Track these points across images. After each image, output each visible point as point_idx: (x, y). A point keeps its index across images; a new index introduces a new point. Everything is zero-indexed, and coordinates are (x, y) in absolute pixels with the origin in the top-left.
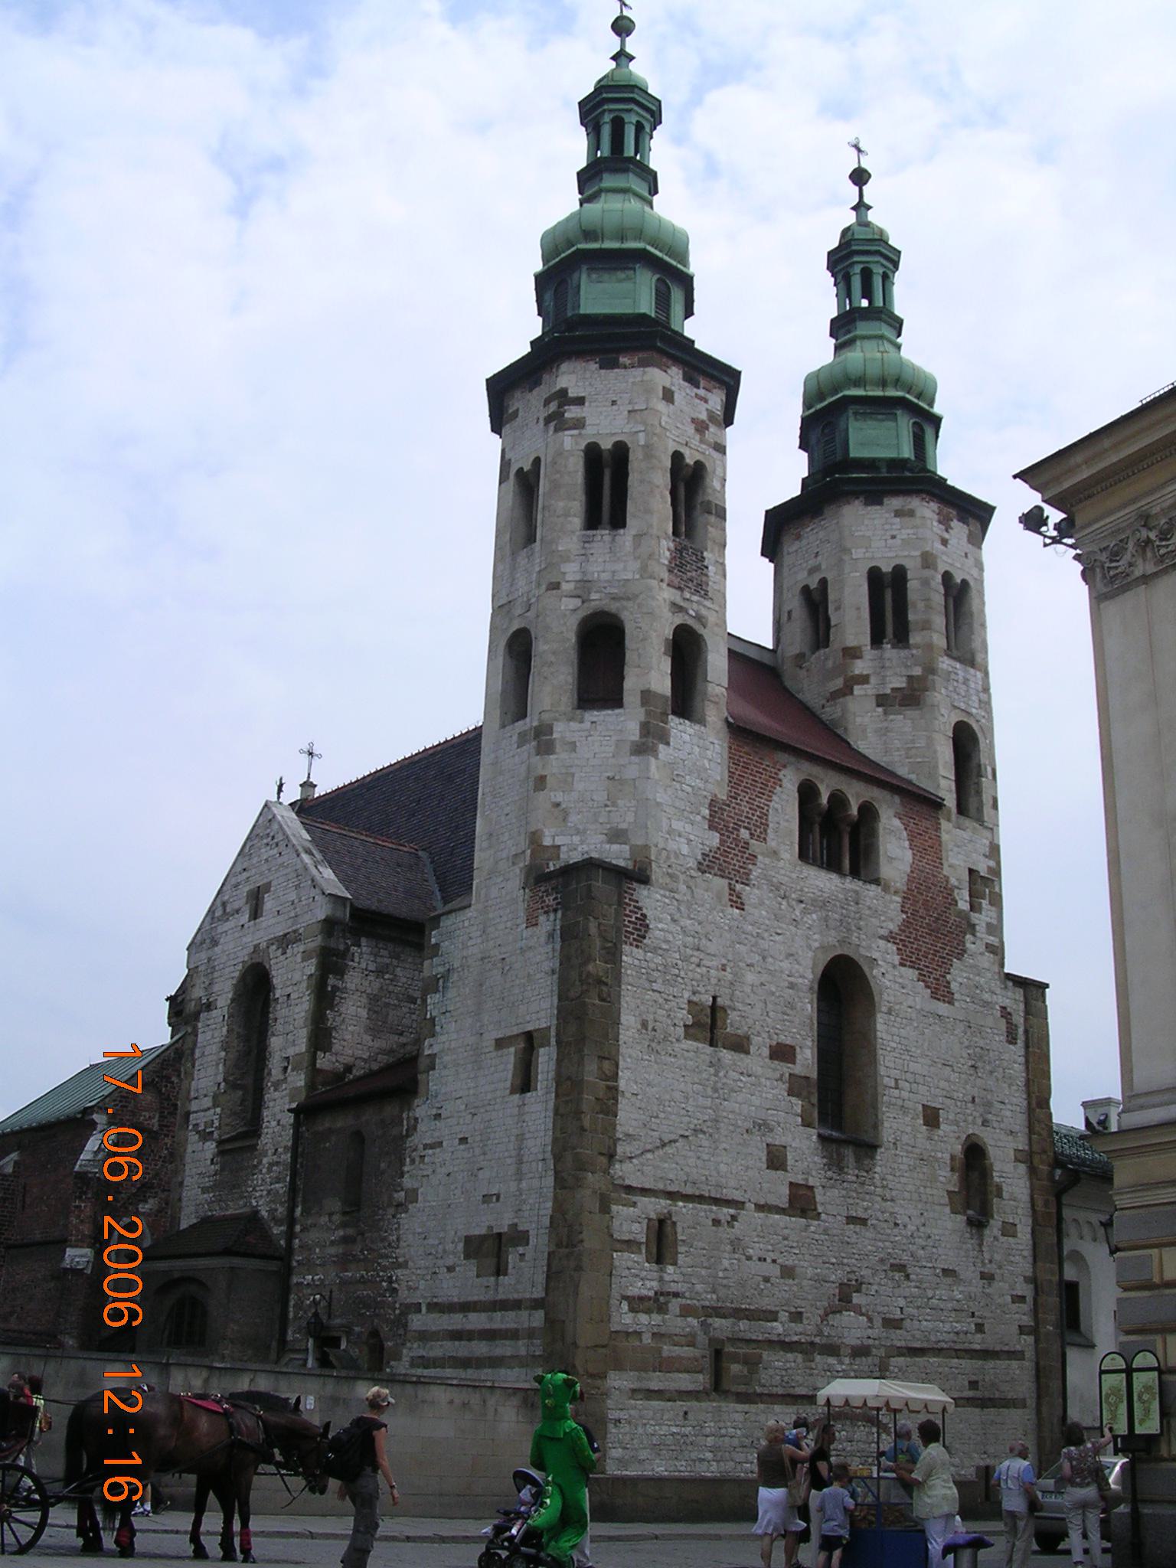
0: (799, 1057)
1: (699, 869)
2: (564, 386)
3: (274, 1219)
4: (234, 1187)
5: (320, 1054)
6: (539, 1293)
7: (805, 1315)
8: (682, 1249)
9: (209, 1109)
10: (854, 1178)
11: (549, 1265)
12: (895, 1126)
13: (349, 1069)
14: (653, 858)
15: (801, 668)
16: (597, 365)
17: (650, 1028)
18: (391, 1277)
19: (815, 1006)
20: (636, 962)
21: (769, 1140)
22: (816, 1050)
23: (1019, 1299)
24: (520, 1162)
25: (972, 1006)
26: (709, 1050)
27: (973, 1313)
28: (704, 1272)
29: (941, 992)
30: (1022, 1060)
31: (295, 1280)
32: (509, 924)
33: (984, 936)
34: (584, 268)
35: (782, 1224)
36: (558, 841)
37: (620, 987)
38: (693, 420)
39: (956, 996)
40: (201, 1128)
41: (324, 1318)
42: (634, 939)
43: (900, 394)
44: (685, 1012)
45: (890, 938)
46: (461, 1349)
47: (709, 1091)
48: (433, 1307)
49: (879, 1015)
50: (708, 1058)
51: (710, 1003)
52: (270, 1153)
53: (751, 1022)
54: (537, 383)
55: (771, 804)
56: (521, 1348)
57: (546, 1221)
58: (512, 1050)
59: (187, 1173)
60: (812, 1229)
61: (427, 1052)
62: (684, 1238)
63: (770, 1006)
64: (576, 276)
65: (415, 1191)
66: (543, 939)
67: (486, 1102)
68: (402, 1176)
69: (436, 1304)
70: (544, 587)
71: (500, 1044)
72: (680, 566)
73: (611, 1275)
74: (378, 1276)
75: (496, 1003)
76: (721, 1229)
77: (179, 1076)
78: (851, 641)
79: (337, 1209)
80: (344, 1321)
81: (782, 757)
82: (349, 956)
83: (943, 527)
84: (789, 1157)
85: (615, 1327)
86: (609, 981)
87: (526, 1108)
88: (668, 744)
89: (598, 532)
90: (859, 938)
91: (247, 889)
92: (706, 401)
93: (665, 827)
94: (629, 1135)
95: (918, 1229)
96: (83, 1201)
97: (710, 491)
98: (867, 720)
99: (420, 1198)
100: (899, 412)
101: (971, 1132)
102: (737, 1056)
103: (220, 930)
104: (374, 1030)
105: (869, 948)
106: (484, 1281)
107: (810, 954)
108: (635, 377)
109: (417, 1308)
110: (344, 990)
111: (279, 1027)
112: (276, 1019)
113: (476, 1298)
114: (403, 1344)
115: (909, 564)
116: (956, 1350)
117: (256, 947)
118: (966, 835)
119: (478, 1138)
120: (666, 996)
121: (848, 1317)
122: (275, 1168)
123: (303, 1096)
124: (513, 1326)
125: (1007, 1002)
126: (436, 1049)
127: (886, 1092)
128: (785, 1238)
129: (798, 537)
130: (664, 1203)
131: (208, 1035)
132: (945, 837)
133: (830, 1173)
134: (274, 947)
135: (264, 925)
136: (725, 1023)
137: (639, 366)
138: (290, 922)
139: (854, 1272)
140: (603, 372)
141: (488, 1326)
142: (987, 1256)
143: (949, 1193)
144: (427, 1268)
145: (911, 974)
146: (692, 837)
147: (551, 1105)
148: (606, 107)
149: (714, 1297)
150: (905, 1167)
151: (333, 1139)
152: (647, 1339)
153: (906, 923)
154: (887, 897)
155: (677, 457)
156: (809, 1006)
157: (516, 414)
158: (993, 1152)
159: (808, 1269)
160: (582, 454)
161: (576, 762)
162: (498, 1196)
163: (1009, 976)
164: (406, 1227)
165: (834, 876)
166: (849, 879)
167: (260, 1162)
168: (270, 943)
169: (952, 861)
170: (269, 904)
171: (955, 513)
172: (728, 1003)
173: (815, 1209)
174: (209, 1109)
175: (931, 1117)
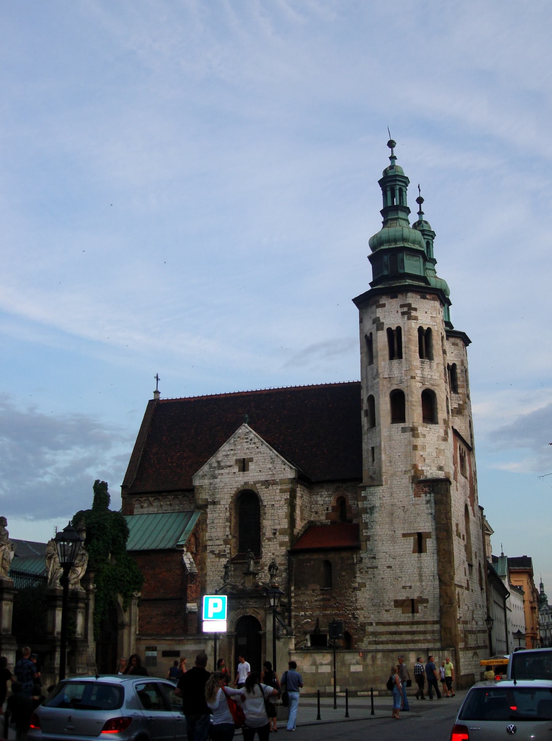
2: (410, 302)
6: (436, 619)
9: (221, 545)
11: (441, 611)
13: (298, 533)
16: (419, 297)
24: (420, 575)
30: (482, 534)
31: (293, 613)
32: (405, 495)
34: (405, 253)
36: (423, 469)
40: (217, 552)
46: (397, 638)
48: (378, 624)
54: (396, 297)
56: (429, 637)
57: (438, 596)
59: (208, 570)
61: (365, 534)
64: (400, 255)
66: (424, 502)
68: (355, 577)
69: (381, 622)
70: (409, 377)
71: (404, 535)
74: (346, 612)
75: (401, 521)
79: (317, 588)
87: (422, 558)
89: (426, 360)
91: (235, 458)
96: (192, 584)
99: (367, 586)
104: (302, 519)
106: (407, 615)
108: (432, 304)
109: (371, 624)
111: (268, 516)
112: (265, 513)
113: (403, 620)
114: (364, 637)
115: (457, 363)
117: (246, 483)
123: (289, 545)
126: (369, 534)
134: (260, 485)
141: (410, 630)
144: (375, 610)
151: (312, 562)
157: (384, 305)
159: (470, 608)
162: (410, 587)
163: (480, 507)
164: (360, 596)
167: (263, 568)
168: (255, 483)
170: (252, 466)
174: (221, 545)
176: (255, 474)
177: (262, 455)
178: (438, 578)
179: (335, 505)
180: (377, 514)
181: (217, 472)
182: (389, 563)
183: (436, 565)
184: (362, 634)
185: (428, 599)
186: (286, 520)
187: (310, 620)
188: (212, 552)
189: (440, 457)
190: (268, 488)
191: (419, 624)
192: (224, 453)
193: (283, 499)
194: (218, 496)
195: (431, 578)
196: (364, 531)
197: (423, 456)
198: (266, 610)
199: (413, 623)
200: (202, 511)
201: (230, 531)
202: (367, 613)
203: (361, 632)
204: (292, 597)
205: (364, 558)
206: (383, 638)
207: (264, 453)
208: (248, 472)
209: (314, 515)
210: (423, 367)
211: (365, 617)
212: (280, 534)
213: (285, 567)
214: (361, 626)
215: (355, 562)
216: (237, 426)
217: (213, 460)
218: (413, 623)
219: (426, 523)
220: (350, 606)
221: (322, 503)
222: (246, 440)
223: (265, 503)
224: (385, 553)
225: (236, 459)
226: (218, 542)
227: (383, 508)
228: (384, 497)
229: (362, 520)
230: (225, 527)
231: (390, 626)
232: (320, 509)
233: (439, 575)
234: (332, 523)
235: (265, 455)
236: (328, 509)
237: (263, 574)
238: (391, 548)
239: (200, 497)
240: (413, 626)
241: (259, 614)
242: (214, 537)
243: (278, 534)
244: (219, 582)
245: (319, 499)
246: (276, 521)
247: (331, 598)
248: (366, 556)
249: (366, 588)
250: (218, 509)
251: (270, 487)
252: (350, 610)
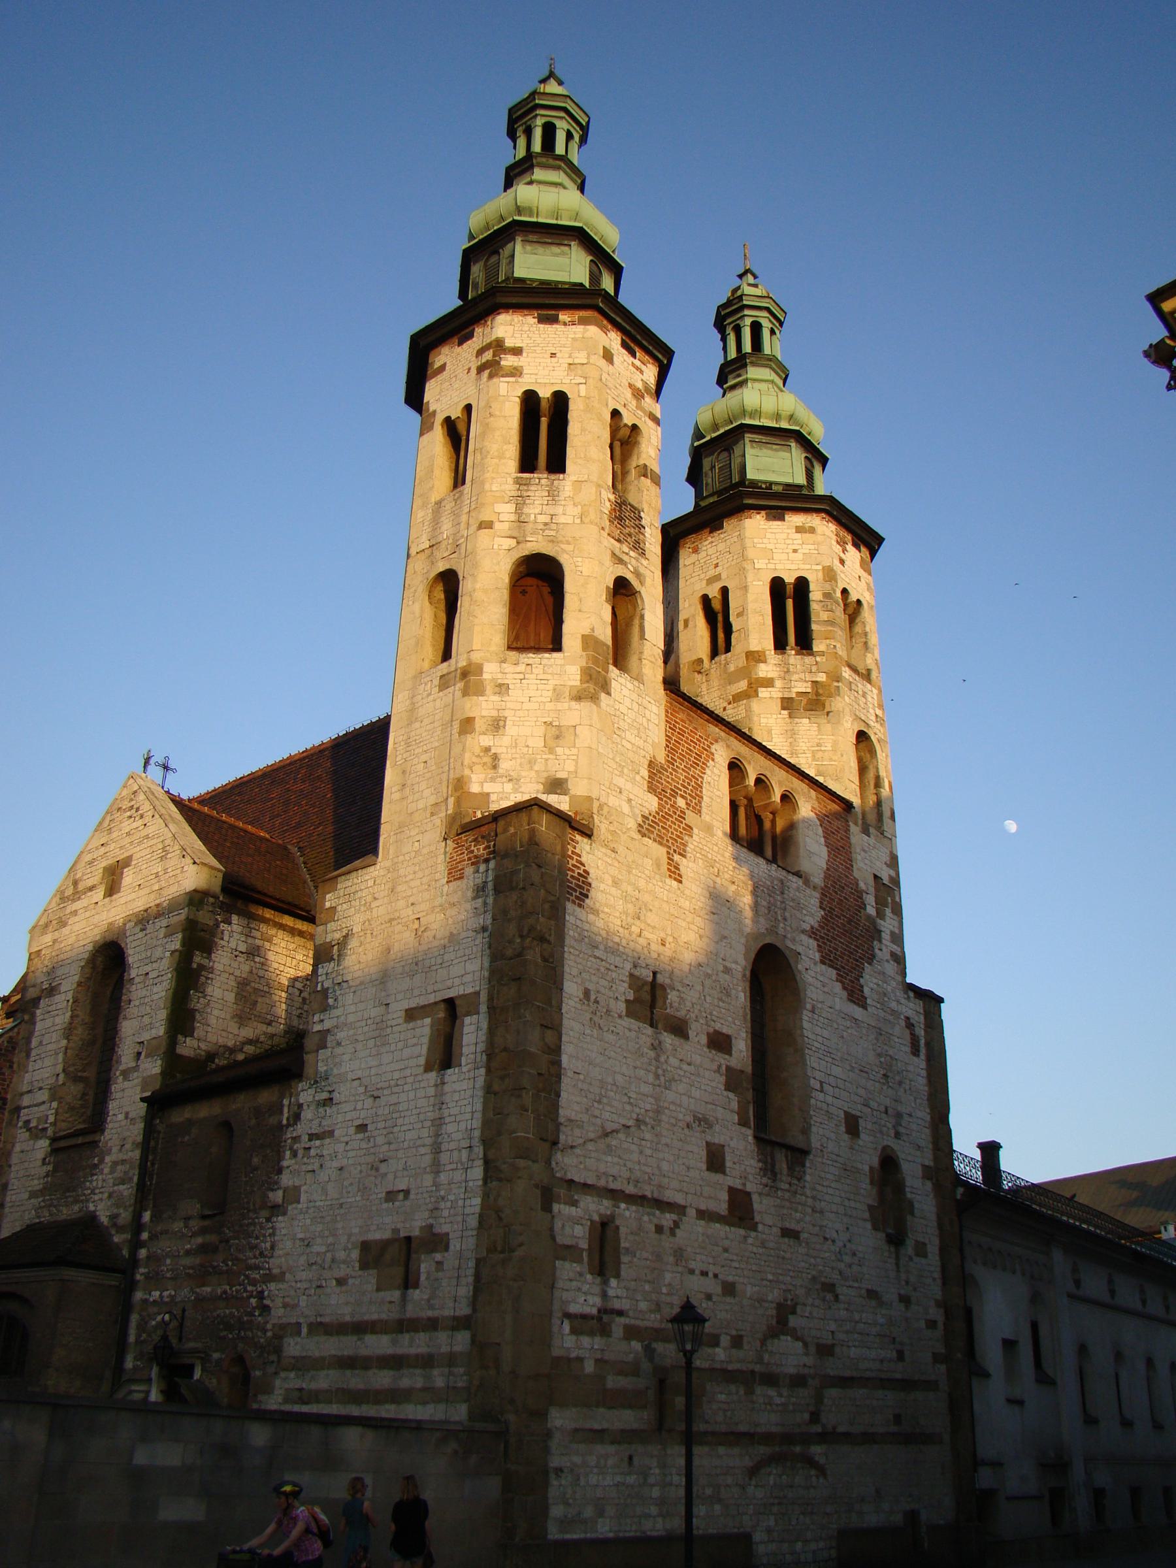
0: (734, 1049)
1: (639, 831)
2: (500, 335)
3: (115, 1225)
5: (180, 1037)
6: (464, 1310)
7: (745, 1339)
8: (625, 1259)
9: (44, 1103)
10: (787, 1186)
11: (477, 1277)
12: (821, 1132)
13: (211, 1056)
14: (595, 811)
15: (699, 672)
16: (536, 320)
17: (593, 997)
18: (262, 1292)
19: (748, 994)
20: (579, 923)
21: (709, 1138)
22: (749, 1042)
23: (932, 1324)
24: (437, 1149)
25: (882, 1014)
26: (649, 1031)
27: (894, 1338)
28: (647, 1287)
29: (856, 996)
30: (924, 1073)
31: (139, 1295)
32: (425, 880)
33: (888, 944)
34: (519, 239)
35: (722, 1234)
36: (488, 788)
37: (563, 947)
38: (630, 386)
39: (869, 1001)
41: (174, 1341)
42: (577, 897)
43: (797, 428)
44: (626, 985)
45: (813, 933)
46: (355, 1381)
47: (651, 1078)
49: (805, 1012)
50: (649, 1041)
51: (650, 979)
52: (115, 1150)
53: (688, 1004)
54: (470, 336)
55: (705, 776)
57: (473, 1222)
58: (428, 1021)
59: (12, 1175)
60: (750, 1240)
61: (317, 1028)
62: (628, 1245)
63: (706, 990)
64: (510, 246)
65: (297, 1189)
67: (393, 1083)
68: (280, 1171)
69: (321, 1323)
71: (411, 1015)
72: (620, 519)
73: (553, 1287)
74: (245, 1290)
76: (664, 1237)
77: (11, 1067)
78: (754, 646)
80: (199, 1345)
81: (714, 730)
82: (219, 936)
83: (841, 549)
84: (728, 1158)
85: (556, 1352)
86: (552, 939)
87: (447, 1088)
88: (609, 694)
89: (536, 475)
90: (785, 929)
91: (104, 864)
92: (642, 372)
93: (607, 784)
94: (570, 1120)
95: (845, 1246)
97: (644, 456)
98: (772, 721)
99: (303, 1198)
100: (793, 444)
101: (885, 1143)
102: (677, 1041)
103: (68, 911)
104: (241, 1018)
105: (793, 940)
107: (743, 940)
108: (575, 333)
110: (211, 970)
111: (132, 1010)
112: (130, 1001)
113: (375, 1317)
114: (276, 1373)
116: (881, 1379)
118: (872, 841)
119: (381, 1125)
120: (608, 966)
121: (785, 1342)
122: (119, 1168)
124: (423, 1350)
125: (910, 1013)
126: (327, 1025)
127: (813, 1095)
128: (726, 1250)
129: (696, 550)
130: (606, 1202)
131: (49, 1023)
132: (853, 840)
133: (765, 1180)
135: (123, 901)
136: (665, 1003)
137: (579, 324)
138: (153, 896)
139: (790, 1291)
140: (542, 326)
141: (390, 1351)
142: (903, 1276)
143: (870, 1207)
144: (310, 1281)
145: (833, 973)
146: (632, 797)
147: (480, 1082)
148: (538, 112)
149: (658, 1317)
150: (831, 1177)
152: (589, 1367)
153: (826, 921)
154: (808, 891)
155: (615, 414)
156: (742, 995)
157: (442, 368)
158: (906, 1167)
160: (518, 400)
161: (509, 705)
162: (407, 1193)
164: (284, 1232)
165: (761, 861)
166: (774, 866)
167: (102, 1161)
169: (861, 865)
170: (129, 878)
171: (849, 538)
172: (667, 981)
173: (753, 1219)
175: (852, 1125)
176: (130, 897)
177: (151, 842)
178: (481, 1155)
180: (354, 957)
182: (363, 1114)
183: (479, 1106)
184: (273, 1362)
185: (448, 1234)
186: (163, 1014)
188: (27, 1122)
189: (559, 750)
191: (416, 1330)
195: (465, 1153)
196: (316, 1018)
197: (493, 751)
199: (404, 1326)
200: (26, 1017)
201: (64, 1060)
202: (292, 1293)
203: (273, 1358)
204: (141, 1244)
205: (305, 1107)
206: (324, 1380)
210: (525, 494)
211: (285, 1306)
212: (147, 1056)
214: (275, 1336)
215: (285, 1122)
218: (404, 1326)
219: (467, 964)
220: (257, 1268)
222: (128, 814)
223: (133, 973)
224: (357, 1082)
225: (105, 869)
227: (369, 935)
228: (375, 899)
229: (317, 983)
231: (342, 1338)
233: (486, 1142)
235: (154, 841)
237: (100, 1177)
238: (375, 1063)
240: (400, 1336)
242: (35, 1084)
244: (23, 1208)
246: (146, 1020)
247: (221, 1242)
248: (310, 1099)
249: (300, 1206)
250: (54, 1007)
251: (150, 928)
252: (254, 1283)
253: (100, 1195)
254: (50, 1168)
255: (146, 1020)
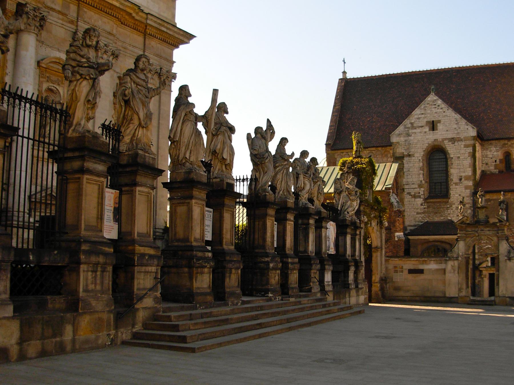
4: (436, 213)
9: (416, 188)
40: (413, 194)
52: (456, 204)
91: (426, 120)
96: (400, 218)
104: (479, 169)
111: (454, 166)
112: (452, 164)
117: (435, 140)
131: (411, 165)
134: (447, 141)
151: (492, 202)
167: (452, 206)
168: (444, 140)
170: (440, 126)
174: (416, 188)
176: (443, 133)
177: (449, 118)
179: (501, 158)
181: (410, 131)
186: (470, 169)
187: (490, 246)
188: (409, 193)
190: (454, 144)
192: (416, 116)
193: (467, 152)
194: (413, 150)
198: (498, 237)
201: (423, 177)
207: (449, 117)
208: (437, 131)
209: (484, 165)
212: (465, 180)
213: (470, 205)
216: (428, 94)
217: (407, 122)
221: (491, 156)
222: (434, 106)
223: (452, 156)
226: (413, 186)
230: (419, 175)
232: (490, 161)
234: (499, 172)
235: (451, 118)
236: (496, 161)
237: (452, 211)
239: (397, 151)
241: (493, 240)
243: (463, 180)
244: (415, 217)
245: (489, 153)
246: (462, 170)
251: (456, 143)
253: (453, 216)
254: (426, 207)
255: (462, 170)
